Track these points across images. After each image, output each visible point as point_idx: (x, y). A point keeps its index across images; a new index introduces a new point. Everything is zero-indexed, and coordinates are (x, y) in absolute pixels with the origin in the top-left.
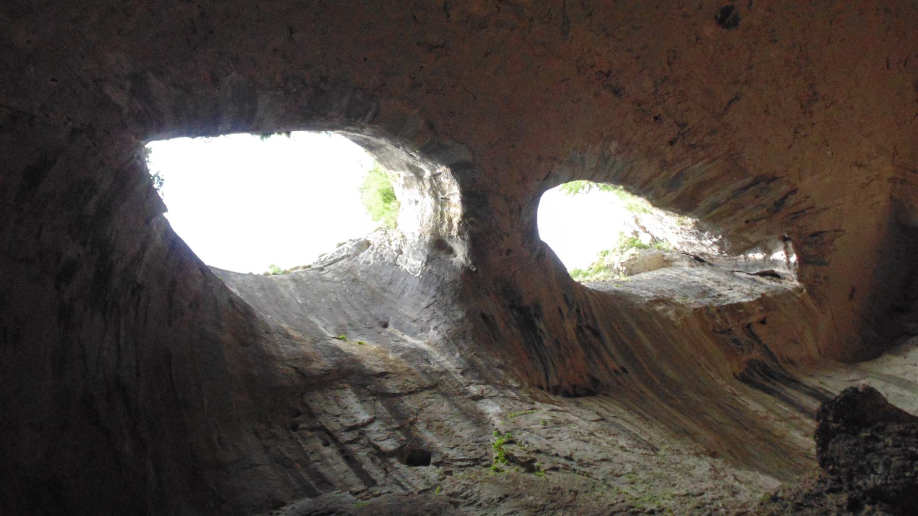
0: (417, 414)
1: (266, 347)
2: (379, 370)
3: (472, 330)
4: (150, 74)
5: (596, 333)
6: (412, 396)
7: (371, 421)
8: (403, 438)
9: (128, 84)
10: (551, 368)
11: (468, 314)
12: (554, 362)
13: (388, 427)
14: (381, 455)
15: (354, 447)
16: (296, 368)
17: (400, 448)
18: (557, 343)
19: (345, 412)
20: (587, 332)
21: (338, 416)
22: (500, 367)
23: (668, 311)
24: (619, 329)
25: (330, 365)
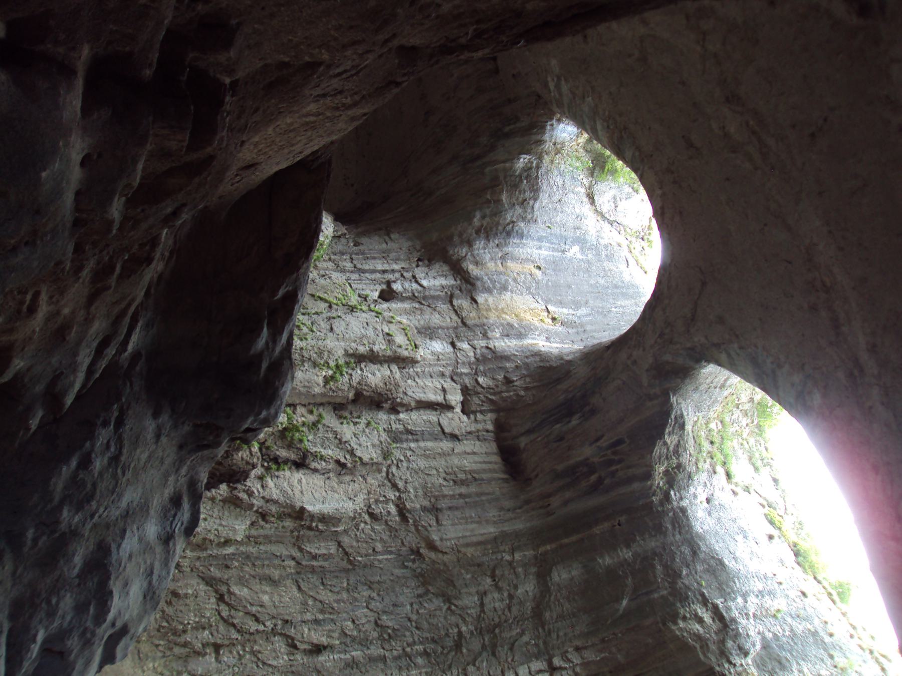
0: (429, 306)
1: (480, 243)
2: (481, 299)
3: (551, 366)
4: (563, 79)
5: (595, 488)
6: (452, 312)
7: (421, 286)
8: (404, 295)
9: (555, 79)
10: (532, 437)
11: (569, 362)
12: (539, 439)
13: (415, 291)
14: (389, 283)
15: (397, 275)
16: (465, 256)
17: (395, 292)
18: (561, 439)
19: (430, 277)
20: (593, 478)
21: (427, 274)
22: (508, 381)
23: (702, 627)
24: (619, 525)
25: (475, 274)
